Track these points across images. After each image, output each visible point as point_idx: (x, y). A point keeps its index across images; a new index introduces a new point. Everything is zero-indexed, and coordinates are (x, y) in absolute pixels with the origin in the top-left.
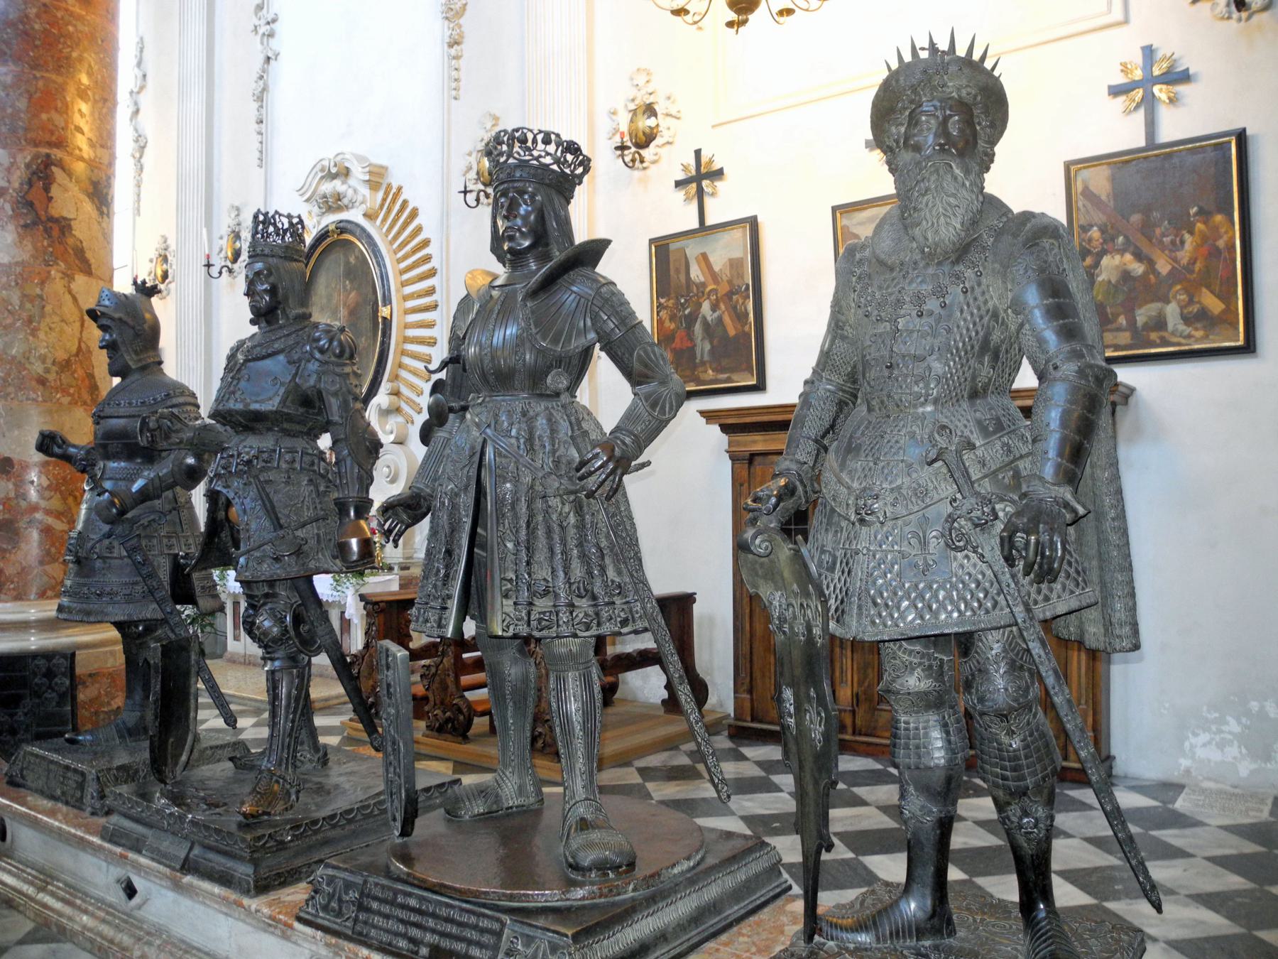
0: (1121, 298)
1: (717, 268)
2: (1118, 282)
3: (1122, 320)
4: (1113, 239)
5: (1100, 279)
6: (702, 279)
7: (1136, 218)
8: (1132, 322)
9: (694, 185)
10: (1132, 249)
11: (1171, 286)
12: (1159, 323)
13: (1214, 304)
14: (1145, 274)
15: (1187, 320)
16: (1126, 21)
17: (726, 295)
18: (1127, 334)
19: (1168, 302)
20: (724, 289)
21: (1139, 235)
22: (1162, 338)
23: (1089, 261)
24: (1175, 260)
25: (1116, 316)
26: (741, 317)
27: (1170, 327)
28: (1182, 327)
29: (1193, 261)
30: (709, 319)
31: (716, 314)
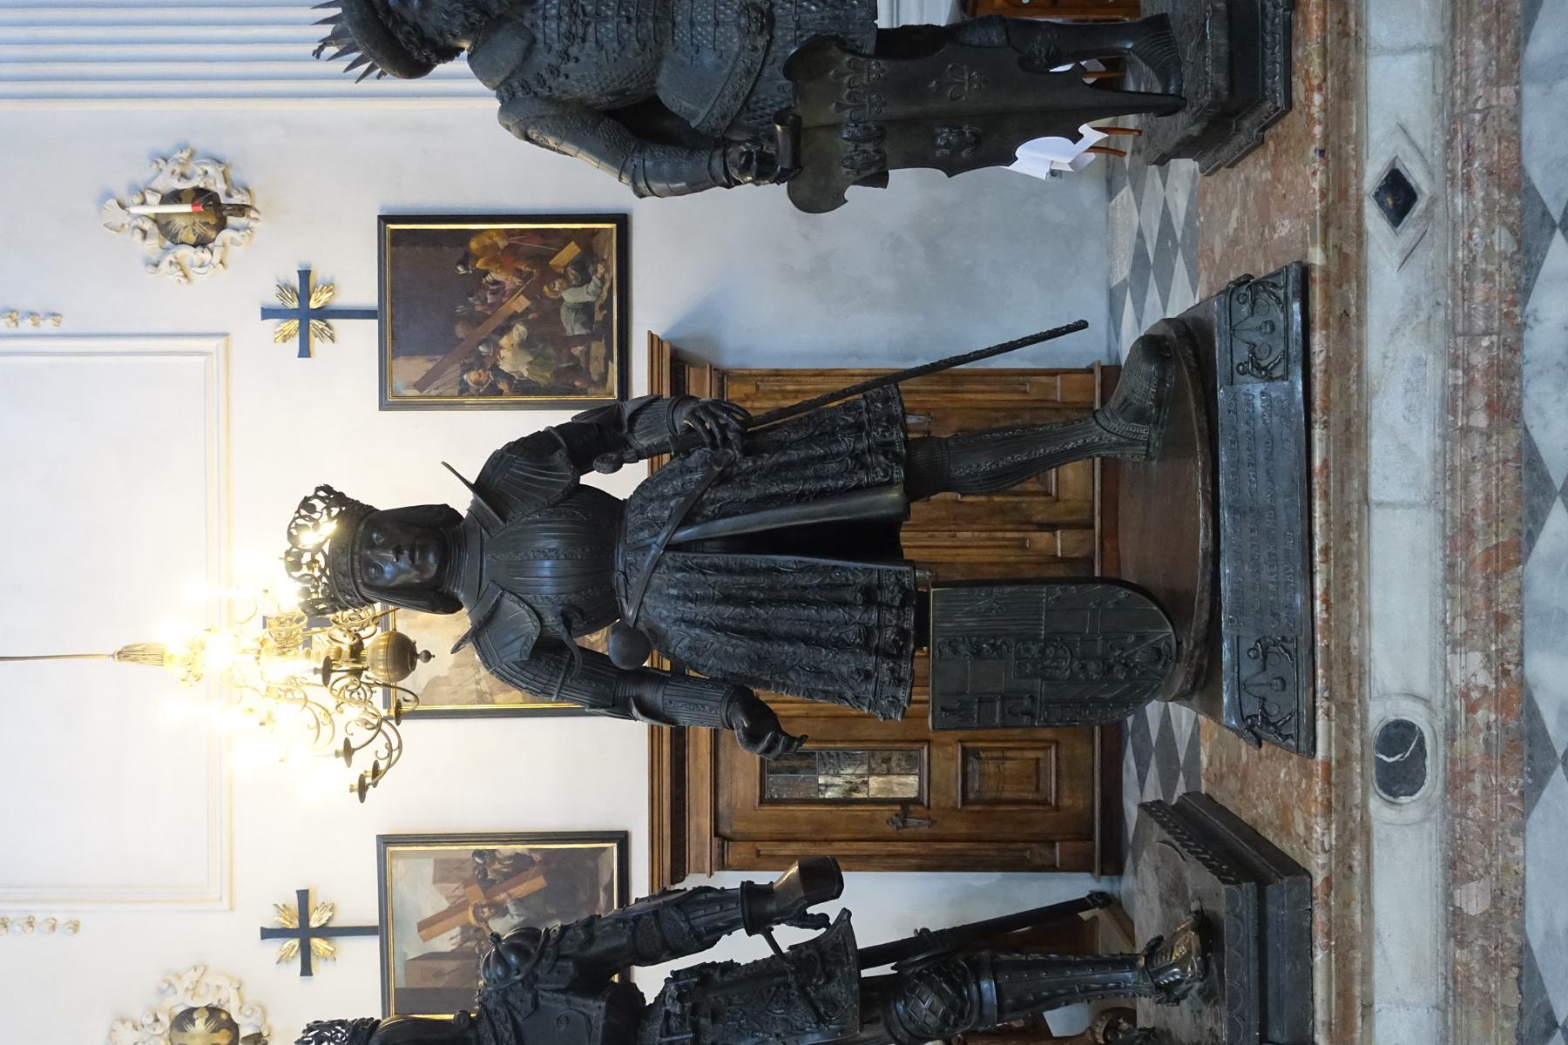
0: (550, 351)
1: (444, 905)
2: (531, 354)
3: (577, 350)
4: (480, 356)
5: (526, 374)
6: (457, 930)
7: (460, 331)
8: (581, 339)
9: (316, 943)
10: (495, 337)
11: (543, 294)
12: (585, 309)
13: (572, 250)
14: (526, 323)
15: (585, 280)
16: (225, 335)
17: (485, 890)
18: (594, 345)
19: (562, 300)
20: (476, 894)
21: (479, 329)
22: (602, 307)
23: (503, 386)
24: (514, 292)
25: (572, 357)
26: (520, 864)
27: (590, 299)
28: (592, 287)
29: (518, 273)
30: (516, 920)
31: (512, 908)
